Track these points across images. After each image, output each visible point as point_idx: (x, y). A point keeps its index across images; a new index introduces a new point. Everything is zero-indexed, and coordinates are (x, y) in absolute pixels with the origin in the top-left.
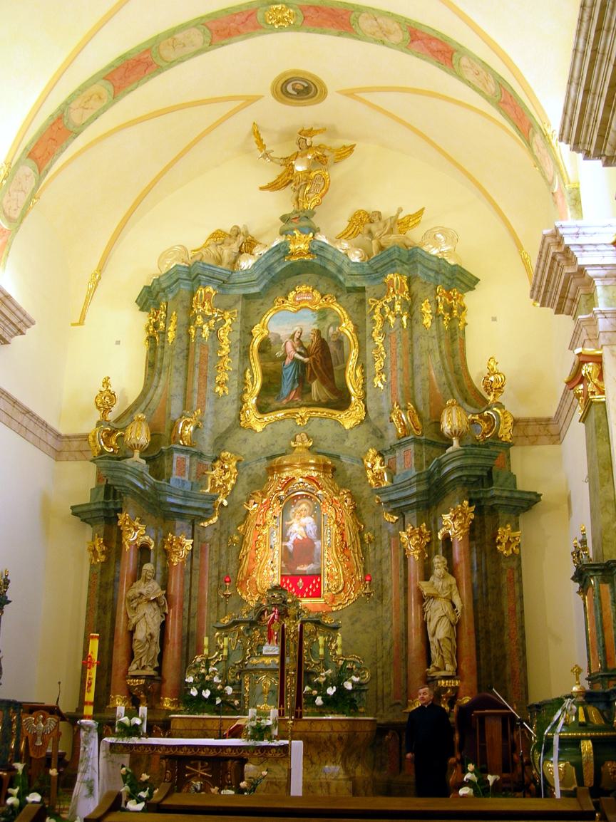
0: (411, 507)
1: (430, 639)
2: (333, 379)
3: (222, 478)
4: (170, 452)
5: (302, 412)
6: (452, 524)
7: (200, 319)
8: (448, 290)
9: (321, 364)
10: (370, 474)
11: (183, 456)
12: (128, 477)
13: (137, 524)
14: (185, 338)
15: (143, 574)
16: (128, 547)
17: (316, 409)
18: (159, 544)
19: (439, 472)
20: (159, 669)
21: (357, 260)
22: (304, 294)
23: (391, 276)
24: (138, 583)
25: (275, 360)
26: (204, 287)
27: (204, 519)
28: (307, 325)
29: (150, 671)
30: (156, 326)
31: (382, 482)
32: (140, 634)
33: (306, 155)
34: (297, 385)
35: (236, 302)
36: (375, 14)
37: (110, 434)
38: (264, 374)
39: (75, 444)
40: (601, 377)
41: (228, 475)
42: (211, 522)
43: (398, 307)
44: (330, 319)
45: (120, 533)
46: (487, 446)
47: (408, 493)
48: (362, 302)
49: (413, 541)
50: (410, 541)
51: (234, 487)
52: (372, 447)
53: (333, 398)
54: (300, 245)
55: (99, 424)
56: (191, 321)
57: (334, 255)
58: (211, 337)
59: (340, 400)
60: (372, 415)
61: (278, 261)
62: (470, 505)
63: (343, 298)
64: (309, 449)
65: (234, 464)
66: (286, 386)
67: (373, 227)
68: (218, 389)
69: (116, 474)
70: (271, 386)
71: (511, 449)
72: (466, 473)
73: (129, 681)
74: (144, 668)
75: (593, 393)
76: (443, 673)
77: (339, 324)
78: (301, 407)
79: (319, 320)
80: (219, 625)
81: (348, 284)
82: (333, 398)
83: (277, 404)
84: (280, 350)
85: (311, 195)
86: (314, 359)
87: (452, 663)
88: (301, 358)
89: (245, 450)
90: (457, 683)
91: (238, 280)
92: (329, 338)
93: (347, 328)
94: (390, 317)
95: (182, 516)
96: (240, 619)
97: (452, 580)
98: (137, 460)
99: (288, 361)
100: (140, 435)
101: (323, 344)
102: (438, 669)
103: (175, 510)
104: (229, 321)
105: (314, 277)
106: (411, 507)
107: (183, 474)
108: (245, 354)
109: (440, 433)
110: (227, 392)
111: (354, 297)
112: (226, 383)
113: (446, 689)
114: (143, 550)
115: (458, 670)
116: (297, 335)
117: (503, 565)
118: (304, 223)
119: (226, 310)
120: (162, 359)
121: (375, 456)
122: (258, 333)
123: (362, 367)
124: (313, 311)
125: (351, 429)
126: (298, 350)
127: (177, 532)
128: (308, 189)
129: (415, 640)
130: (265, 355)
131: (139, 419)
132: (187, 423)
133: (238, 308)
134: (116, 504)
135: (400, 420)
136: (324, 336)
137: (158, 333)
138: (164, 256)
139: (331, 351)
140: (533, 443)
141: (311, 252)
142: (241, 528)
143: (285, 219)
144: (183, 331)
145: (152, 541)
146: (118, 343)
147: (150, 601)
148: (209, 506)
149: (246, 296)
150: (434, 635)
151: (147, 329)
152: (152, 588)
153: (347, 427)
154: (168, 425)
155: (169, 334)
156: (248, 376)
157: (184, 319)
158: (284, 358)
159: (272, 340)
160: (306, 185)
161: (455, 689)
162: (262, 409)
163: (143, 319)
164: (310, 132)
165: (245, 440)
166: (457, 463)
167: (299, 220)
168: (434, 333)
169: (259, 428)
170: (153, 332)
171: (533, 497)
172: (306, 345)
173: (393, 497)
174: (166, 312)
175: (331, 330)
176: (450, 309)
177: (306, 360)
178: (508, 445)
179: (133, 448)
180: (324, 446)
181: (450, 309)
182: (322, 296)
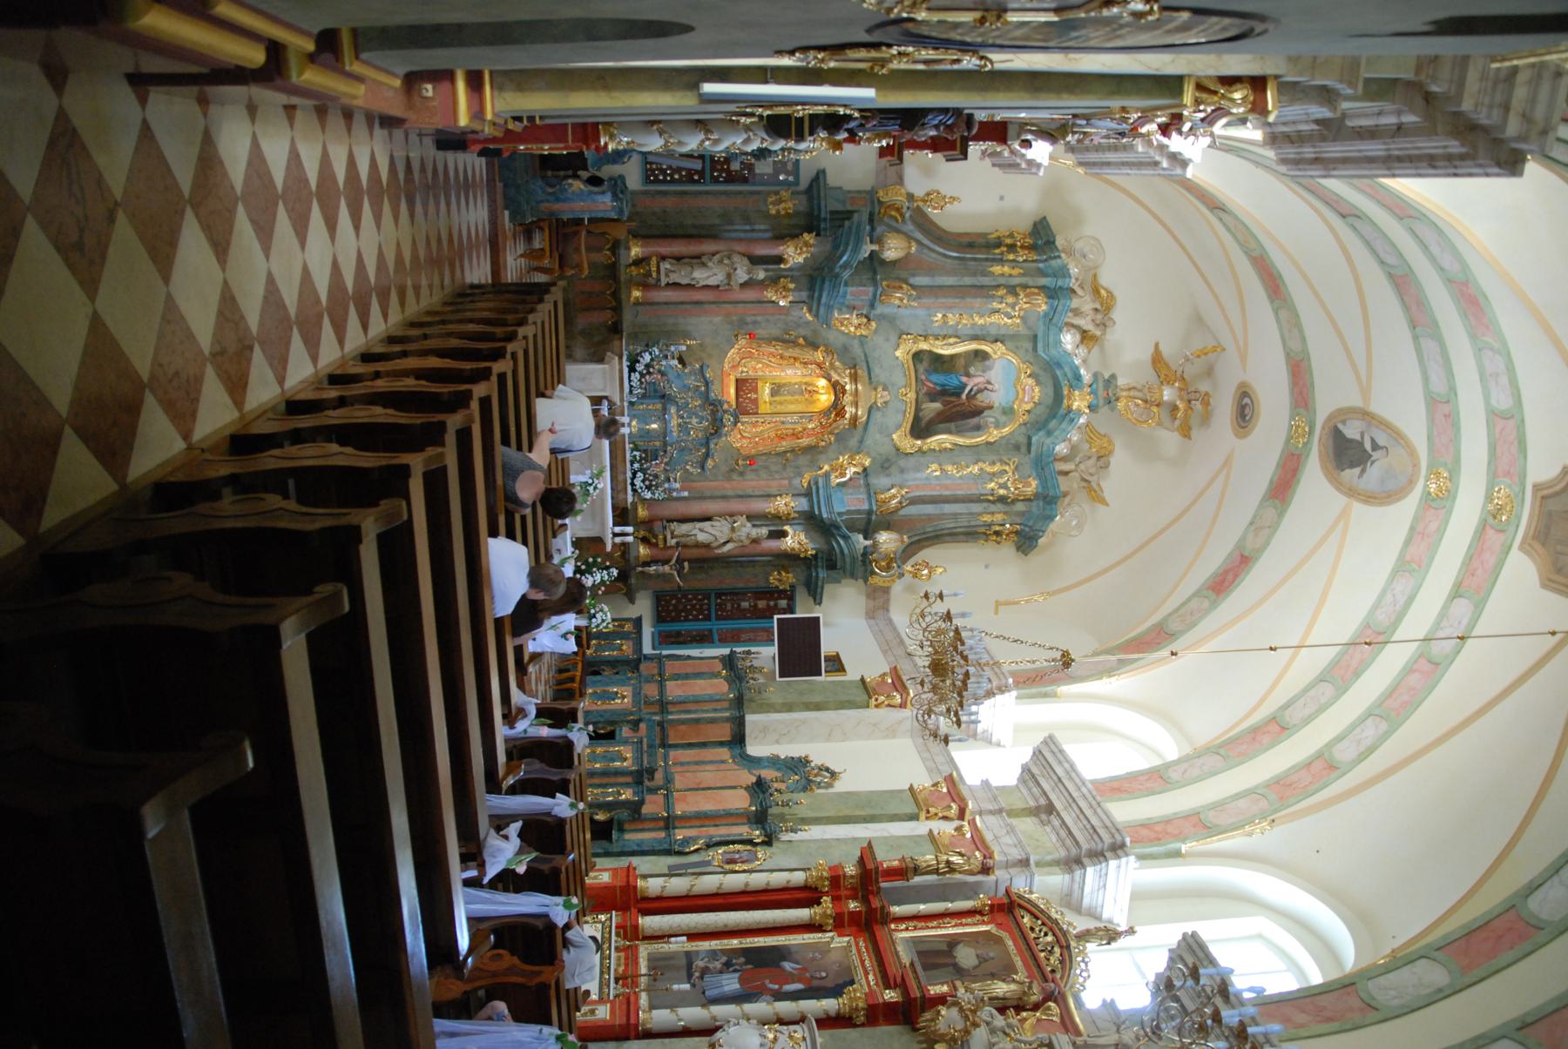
0: (812, 506)
2: (941, 422)
4: (875, 283)
5: (912, 395)
6: (795, 540)
7: (1010, 300)
8: (1017, 533)
9: (958, 412)
11: (870, 294)
13: (804, 256)
16: (782, 248)
17: (913, 409)
18: (786, 273)
19: (840, 535)
20: (668, 284)
22: (1032, 394)
24: (746, 261)
25: (966, 367)
27: (810, 311)
28: (998, 397)
29: (663, 282)
30: (1012, 248)
31: (837, 474)
33: (1181, 399)
34: (938, 388)
36: (1274, 527)
38: (953, 357)
40: (889, 705)
43: (1002, 492)
44: (1003, 419)
45: (794, 236)
46: (864, 562)
47: (823, 510)
48: (1017, 447)
50: (782, 504)
52: (873, 462)
53: (923, 423)
54: (1079, 402)
55: (910, 197)
56: (1012, 290)
57: (1064, 430)
59: (921, 429)
60: (902, 463)
61: (1066, 375)
63: (1023, 429)
64: (875, 403)
65: (864, 333)
66: (938, 378)
67: (1093, 460)
68: (940, 315)
69: (852, 238)
70: (940, 363)
71: (861, 581)
72: (839, 556)
73: (654, 259)
74: (667, 275)
75: (876, 700)
76: (669, 537)
78: (917, 393)
79: (1003, 408)
80: (705, 368)
82: (923, 423)
83: (921, 369)
84: (977, 371)
85: (1132, 407)
86: (964, 404)
88: (966, 391)
91: (1051, 333)
92: (984, 418)
93: (994, 435)
94: (993, 485)
95: (811, 297)
97: (747, 542)
98: (868, 248)
99: (964, 379)
100: (893, 250)
101: (978, 412)
102: (672, 533)
103: (816, 294)
105: (1050, 401)
106: (812, 506)
107: (852, 294)
108: (975, 338)
109: (876, 531)
110: (937, 324)
111: (1023, 440)
112: (945, 323)
114: (779, 260)
115: (671, 547)
116: (989, 387)
118: (1101, 402)
119: (1022, 318)
121: (863, 465)
122: (996, 350)
123: (951, 449)
124: (1014, 402)
126: (975, 388)
127: (796, 294)
128: (1140, 402)
130: (973, 356)
131: (910, 247)
132: (901, 299)
133: (1023, 330)
134: (825, 229)
135: (894, 497)
136: (985, 413)
137: (1002, 254)
139: (969, 421)
141: (1069, 410)
142: (801, 341)
143: (1113, 377)
145: (788, 266)
146: (1002, 198)
147: (729, 276)
149: (1035, 337)
150: (701, 530)
151: (1011, 235)
152: (742, 275)
153: (894, 436)
154: (903, 274)
155: (999, 268)
156: (952, 340)
158: (968, 375)
159: (987, 363)
160: (1146, 401)
161: (656, 545)
162: (918, 356)
163: (1024, 225)
164: (1206, 403)
165: (888, 340)
166: (846, 551)
167: (1107, 392)
168: (973, 523)
169: (898, 353)
170: (1007, 245)
171: (818, 601)
172: (979, 396)
173: (821, 492)
174: (1025, 261)
175: (992, 420)
177: (964, 396)
178: (866, 581)
179: (878, 241)
180: (877, 416)
181: (997, 533)
182: (1028, 411)
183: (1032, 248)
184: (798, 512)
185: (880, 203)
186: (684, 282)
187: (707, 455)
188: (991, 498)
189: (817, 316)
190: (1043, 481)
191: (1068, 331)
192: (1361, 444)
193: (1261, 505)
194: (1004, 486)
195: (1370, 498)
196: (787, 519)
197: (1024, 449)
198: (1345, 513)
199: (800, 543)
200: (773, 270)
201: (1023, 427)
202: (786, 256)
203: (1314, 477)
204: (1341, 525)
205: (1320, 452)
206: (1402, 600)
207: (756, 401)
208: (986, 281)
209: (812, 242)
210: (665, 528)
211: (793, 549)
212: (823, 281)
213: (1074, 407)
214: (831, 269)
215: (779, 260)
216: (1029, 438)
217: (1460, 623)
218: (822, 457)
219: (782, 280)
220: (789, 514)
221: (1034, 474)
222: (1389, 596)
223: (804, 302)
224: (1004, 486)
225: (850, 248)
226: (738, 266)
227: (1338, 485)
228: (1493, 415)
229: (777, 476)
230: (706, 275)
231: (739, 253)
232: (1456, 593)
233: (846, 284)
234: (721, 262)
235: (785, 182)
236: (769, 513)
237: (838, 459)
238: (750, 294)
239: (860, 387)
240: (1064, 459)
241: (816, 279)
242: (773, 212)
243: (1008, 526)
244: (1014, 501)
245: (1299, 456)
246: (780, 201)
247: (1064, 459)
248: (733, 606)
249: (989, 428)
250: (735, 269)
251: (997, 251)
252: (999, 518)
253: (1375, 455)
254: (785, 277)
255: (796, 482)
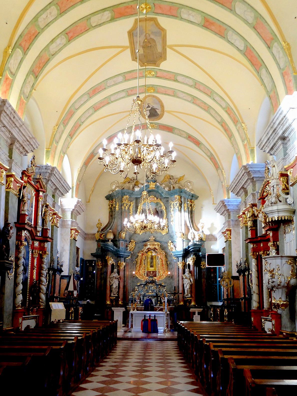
1: (185, 288)
3: (131, 246)
4: (119, 240)
6: (190, 261)
7: (125, 205)
8: (191, 200)
10: (169, 247)
11: (122, 241)
12: (110, 248)
13: (111, 259)
14: (121, 209)
15: (114, 271)
16: (109, 265)
18: (117, 264)
19: (188, 249)
20: (118, 295)
21: (167, 190)
23: (177, 196)
24: (113, 274)
26: (126, 196)
27: (127, 257)
29: (116, 295)
30: (112, 205)
32: (114, 286)
35: (134, 199)
37: (101, 235)
39: (90, 236)
41: (133, 246)
42: (129, 258)
44: (159, 205)
47: (180, 253)
48: (168, 201)
49: (181, 264)
50: (180, 265)
51: (134, 248)
55: (98, 232)
58: (128, 209)
60: (170, 232)
62: (195, 257)
73: (111, 298)
74: (115, 294)
77: (161, 207)
81: (164, 197)
87: (190, 294)
89: (137, 239)
90: (191, 298)
93: (164, 208)
95: (123, 257)
96: (142, 284)
97: (190, 275)
98: (110, 243)
100: (110, 236)
102: (187, 295)
103: (122, 256)
104: (132, 205)
113: (189, 300)
115: (191, 296)
117: (202, 271)
120: (115, 215)
121: (171, 243)
124: (154, 203)
125: (164, 235)
127: (122, 261)
129: (181, 289)
133: (134, 202)
136: (157, 210)
137: (113, 208)
138: (112, 184)
140: (210, 241)
142: (136, 259)
144: (120, 207)
145: (115, 263)
147: (116, 278)
148: (129, 254)
149: (136, 198)
151: (109, 205)
152: (115, 275)
153: (163, 234)
154: (118, 233)
155: (117, 208)
157: (120, 204)
163: (107, 202)
165: (137, 237)
170: (111, 206)
174: (115, 202)
176: (191, 205)
179: (109, 239)
181: (191, 205)
182: (157, 199)
183: (112, 200)
184: (182, 261)
185: (99, 239)
186: (117, 290)
187: (161, 285)
188: (180, 208)
189: (129, 256)
190: (175, 193)
191: (134, 189)
192: (150, 110)
193: (175, 134)
194: (176, 204)
195: (162, 106)
196: (185, 263)
197: (167, 199)
198: (169, 112)
199: (191, 260)
200: (116, 267)
201: (162, 200)
202: (112, 264)
203: (165, 120)
204: (172, 113)
205: (157, 120)
206: (184, 95)
207: (153, 272)
208: (120, 212)
209: (108, 257)
210: (186, 297)
211: (193, 262)
212: (118, 254)
213: (154, 186)
214: (115, 252)
215: (113, 265)
216: (164, 198)
217: (184, 79)
218: (169, 254)
219: (118, 264)
220: (183, 263)
221: (174, 196)
222: (184, 98)
223: (125, 259)
224: (176, 204)
225: (109, 247)
226: (113, 276)
227: (163, 115)
228: (126, 80)
229: (174, 266)
230: (115, 285)
231: (110, 275)
232: (176, 81)
233: (119, 248)
234: (112, 280)
235: (95, 263)
236: (183, 268)
237: (169, 249)
238: (122, 273)
239: (148, 244)
240: (170, 188)
241: (117, 256)
242: (101, 267)
243: (188, 202)
244: (181, 201)
245: (159, 125)
246: (98, 265)
247: (170, 188)
248: (213, 279)
249: (161, 209)
250: (114, 276)
251: (113, 209)
252: (186, 205)
253: (151, 107)
254: (118, 264)
255: (175, 261)
